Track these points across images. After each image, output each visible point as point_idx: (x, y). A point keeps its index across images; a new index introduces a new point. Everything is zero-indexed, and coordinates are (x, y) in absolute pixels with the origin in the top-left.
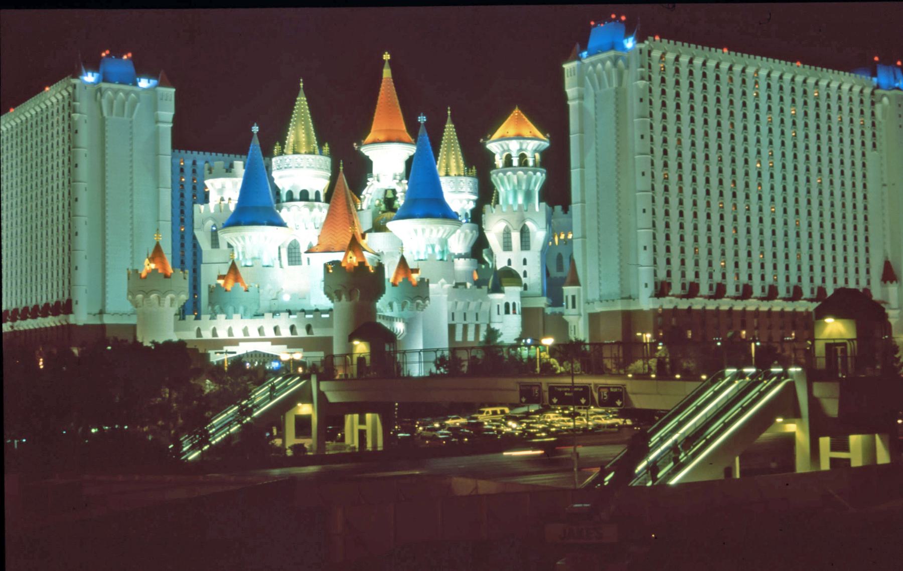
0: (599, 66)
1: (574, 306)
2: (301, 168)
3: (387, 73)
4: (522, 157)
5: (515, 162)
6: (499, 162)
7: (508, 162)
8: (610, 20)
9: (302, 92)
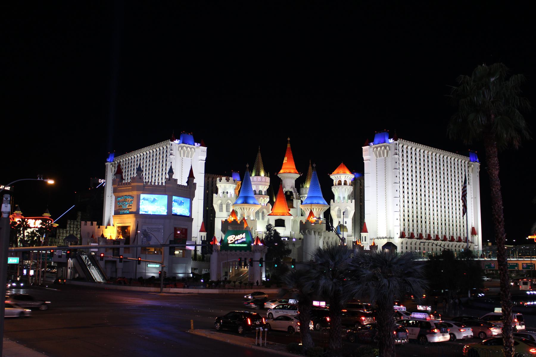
0: (379, 148)
1: (365, 241)
2: (260, 182)
3: (289, 146)
4: (345, 181)
5: (343, 184)
6: (335, 182)
7: (340, 184)
8: (384, 131)
9: (259, 151)
